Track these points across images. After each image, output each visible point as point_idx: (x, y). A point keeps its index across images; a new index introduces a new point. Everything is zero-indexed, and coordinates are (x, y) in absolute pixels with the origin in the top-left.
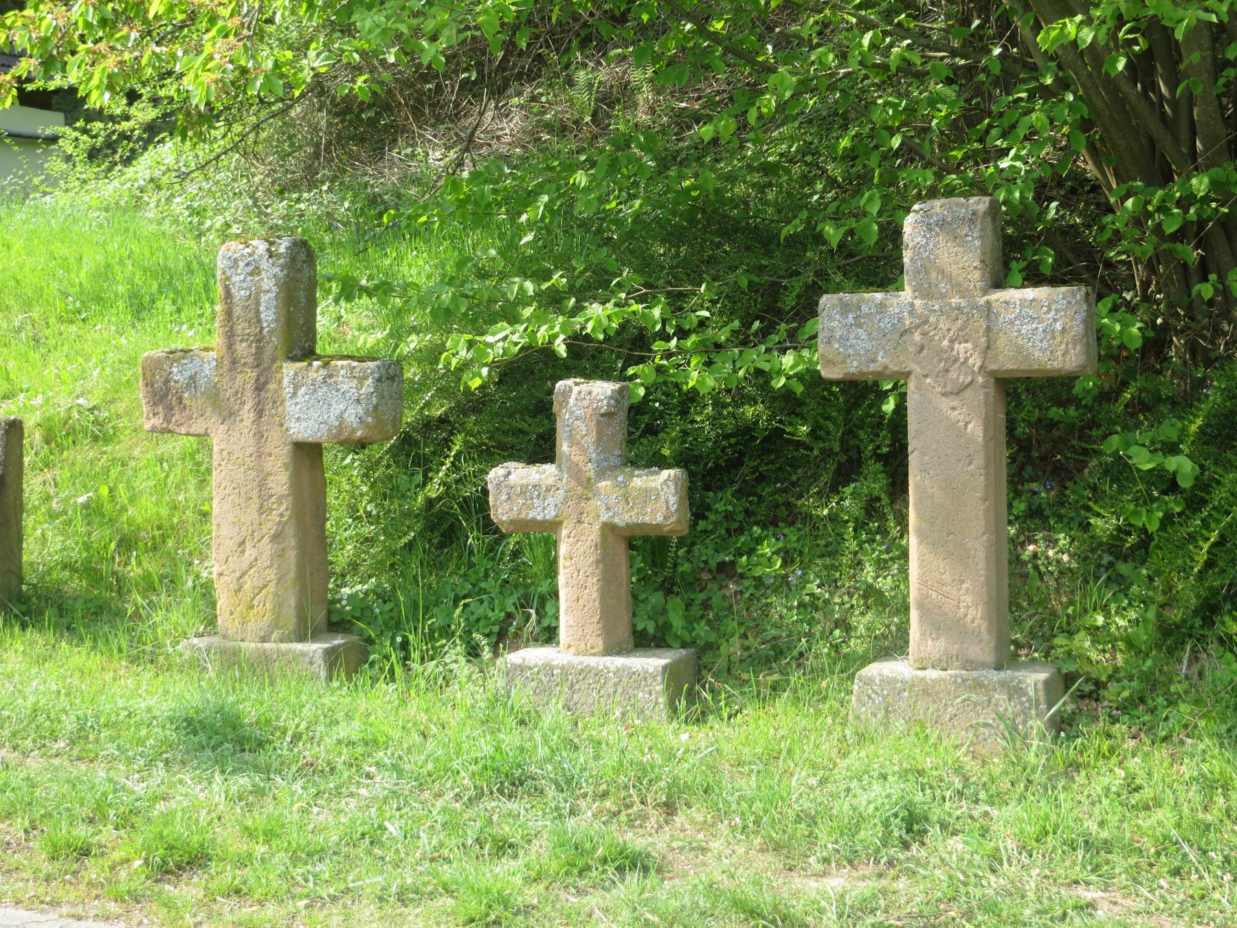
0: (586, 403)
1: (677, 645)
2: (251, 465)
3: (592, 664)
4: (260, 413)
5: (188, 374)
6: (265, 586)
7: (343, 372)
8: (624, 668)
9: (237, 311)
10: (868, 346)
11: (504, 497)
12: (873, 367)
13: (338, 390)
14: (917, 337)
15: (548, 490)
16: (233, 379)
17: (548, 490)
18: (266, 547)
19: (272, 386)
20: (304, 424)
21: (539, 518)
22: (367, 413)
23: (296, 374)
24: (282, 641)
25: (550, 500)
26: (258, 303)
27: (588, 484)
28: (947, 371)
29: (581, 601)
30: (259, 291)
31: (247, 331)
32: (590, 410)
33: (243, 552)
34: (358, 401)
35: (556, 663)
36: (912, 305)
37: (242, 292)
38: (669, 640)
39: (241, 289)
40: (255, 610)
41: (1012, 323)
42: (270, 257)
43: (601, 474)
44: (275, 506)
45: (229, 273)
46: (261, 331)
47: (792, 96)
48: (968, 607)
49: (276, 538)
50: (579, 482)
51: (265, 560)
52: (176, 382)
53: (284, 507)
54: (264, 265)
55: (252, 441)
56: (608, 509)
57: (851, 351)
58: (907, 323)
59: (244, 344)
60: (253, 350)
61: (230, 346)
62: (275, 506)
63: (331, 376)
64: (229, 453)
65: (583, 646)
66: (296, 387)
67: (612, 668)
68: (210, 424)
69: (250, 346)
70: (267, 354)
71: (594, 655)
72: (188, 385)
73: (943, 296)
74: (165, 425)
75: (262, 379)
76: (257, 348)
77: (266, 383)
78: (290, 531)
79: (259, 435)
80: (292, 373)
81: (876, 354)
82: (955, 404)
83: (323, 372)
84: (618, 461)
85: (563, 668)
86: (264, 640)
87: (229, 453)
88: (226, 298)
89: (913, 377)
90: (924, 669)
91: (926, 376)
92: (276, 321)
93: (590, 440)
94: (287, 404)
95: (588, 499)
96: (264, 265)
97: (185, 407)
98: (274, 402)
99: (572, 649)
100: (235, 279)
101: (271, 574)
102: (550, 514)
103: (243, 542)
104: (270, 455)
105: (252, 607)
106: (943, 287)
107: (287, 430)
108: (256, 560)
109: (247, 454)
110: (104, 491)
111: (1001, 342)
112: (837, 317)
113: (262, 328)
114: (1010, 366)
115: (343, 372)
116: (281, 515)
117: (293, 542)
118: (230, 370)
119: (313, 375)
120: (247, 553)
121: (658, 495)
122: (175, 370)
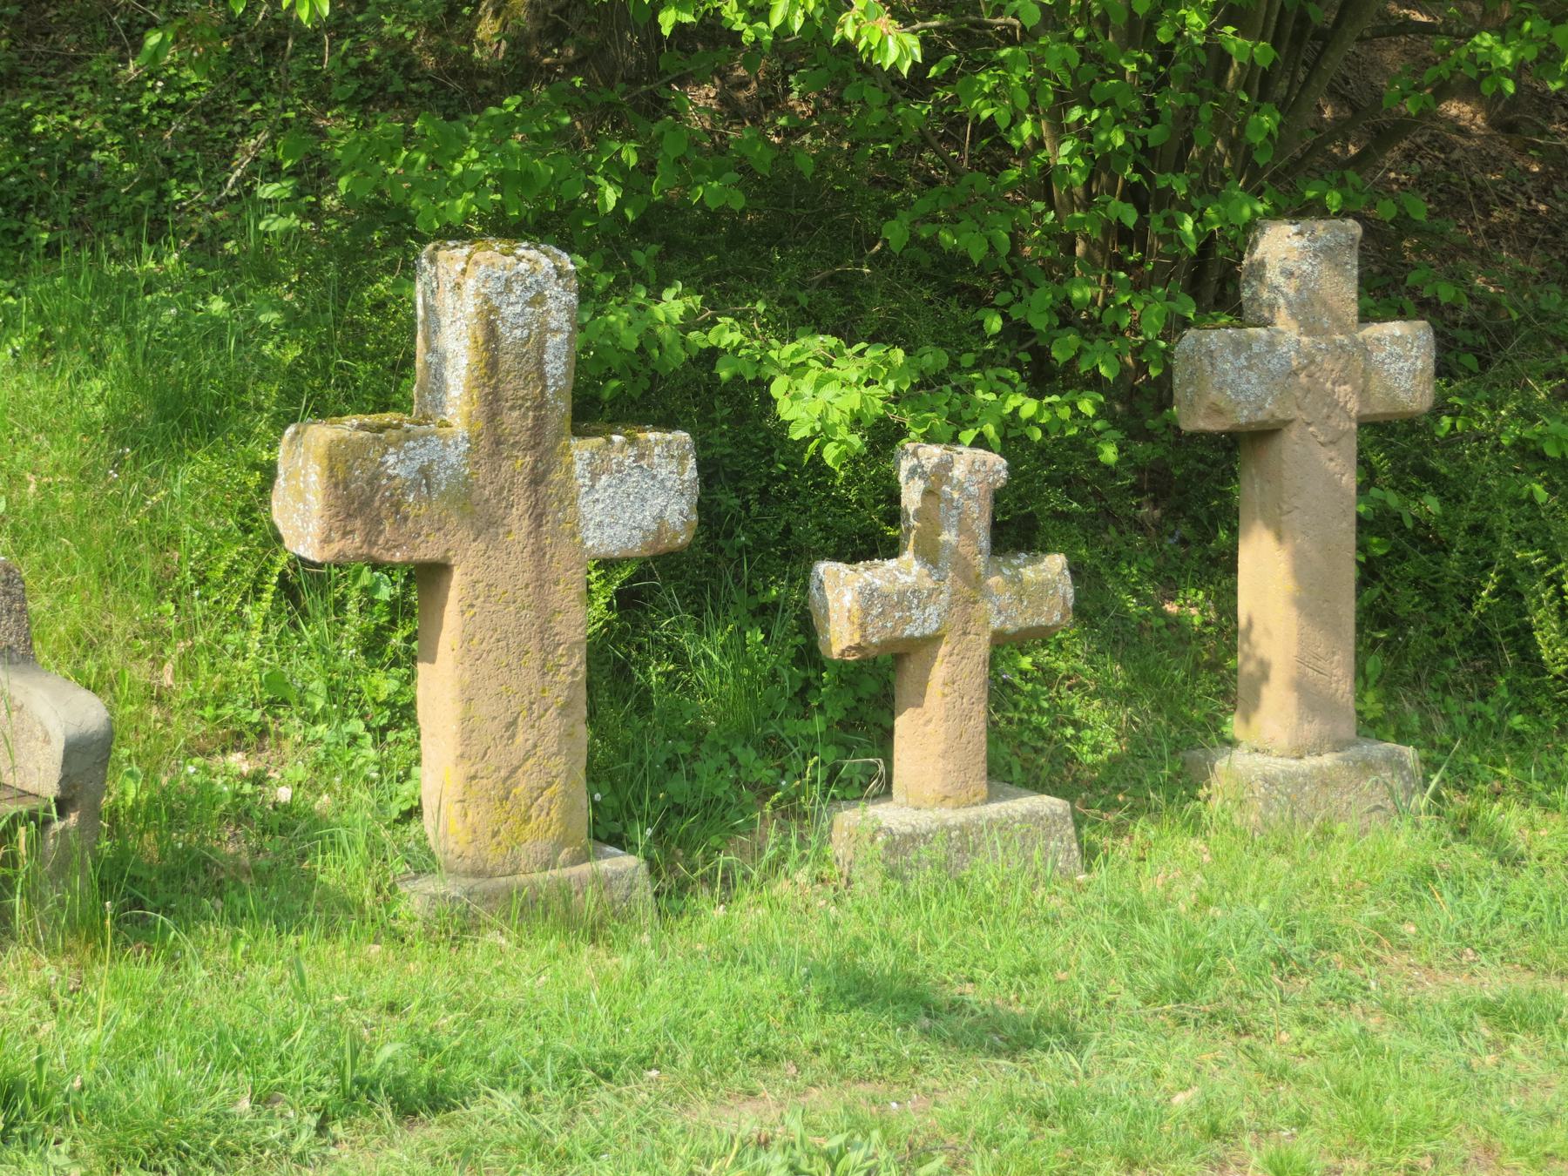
0: (981, 476)
2: (527, 601)
4: (538, 519)
5: (416, 464)
6: (550, 785)
7: (657, 450)
9: (507, 361)
10: (1258, 390)
12: (1261, 416)
13: (654, 477)
14: (1303, 378)
15: (930, 596)
16: (496, 469)
18: (552, 723)
19: (556, 476)
20: (609, 532)
21: (917, 634)
23: (593, 455)
25: (930, 609)
27: (976, 583)
28: (1329, 417)
29: (964, 740)
30: (545, 329)
31: (521, 393)
33: (512, 737)
36: (1299, 342)
37: (518, 332)
39: (514, 326)
40: (533, 824)
41: (1383, 362)
42: (560, 276)
44: (563, 661)
45: (495, 302)
46: (542, 392)
47: (246, 9)
48: (1338, 682)
49: (565, 709)
50: (966, 580)
51: (550, 743)
52: (390, 478)
53: (577, 659)
54: (553, 289)
57: (1242, 398)
58: (1294, 363)
59: (516, 414)
60: (530, 422)
62: (563, 661)
63: (641, 456)
64: (489, 586)
66: (595, 477)
68: (453, 542)
69: (525, 416)
70: (549, 429)
72: (416, 485)
73: (1326, 332)
74: (365, 550)
76: (536, 418)
79: (539, 552)
80: (587, 455)
81: (1265, 400)
82: (1333, 454)
83: (632, 451)
85: (961, 828)
86: (546, 866)
87: (489, 586)
88: (487, 342)
89: (1296, 425)
90: (1301, 757)
91: (1309, 424)
92: (566, 375)
95: (975, 602)
97: (406, 519)
98: (561, 501)
99: (950, 802)
100: (507, 311)
102: (931, 627)
104: (557, 583)
106: (1326, 321)
107: (583, 542)
108: (535, 746)
109: (520, 584)
111: (1375, 382)
112: (1231, 358)
113: (545, 387)
114: (1380, 410)
116: (574, 673)
120: (519, 739)
122: (391, 460)
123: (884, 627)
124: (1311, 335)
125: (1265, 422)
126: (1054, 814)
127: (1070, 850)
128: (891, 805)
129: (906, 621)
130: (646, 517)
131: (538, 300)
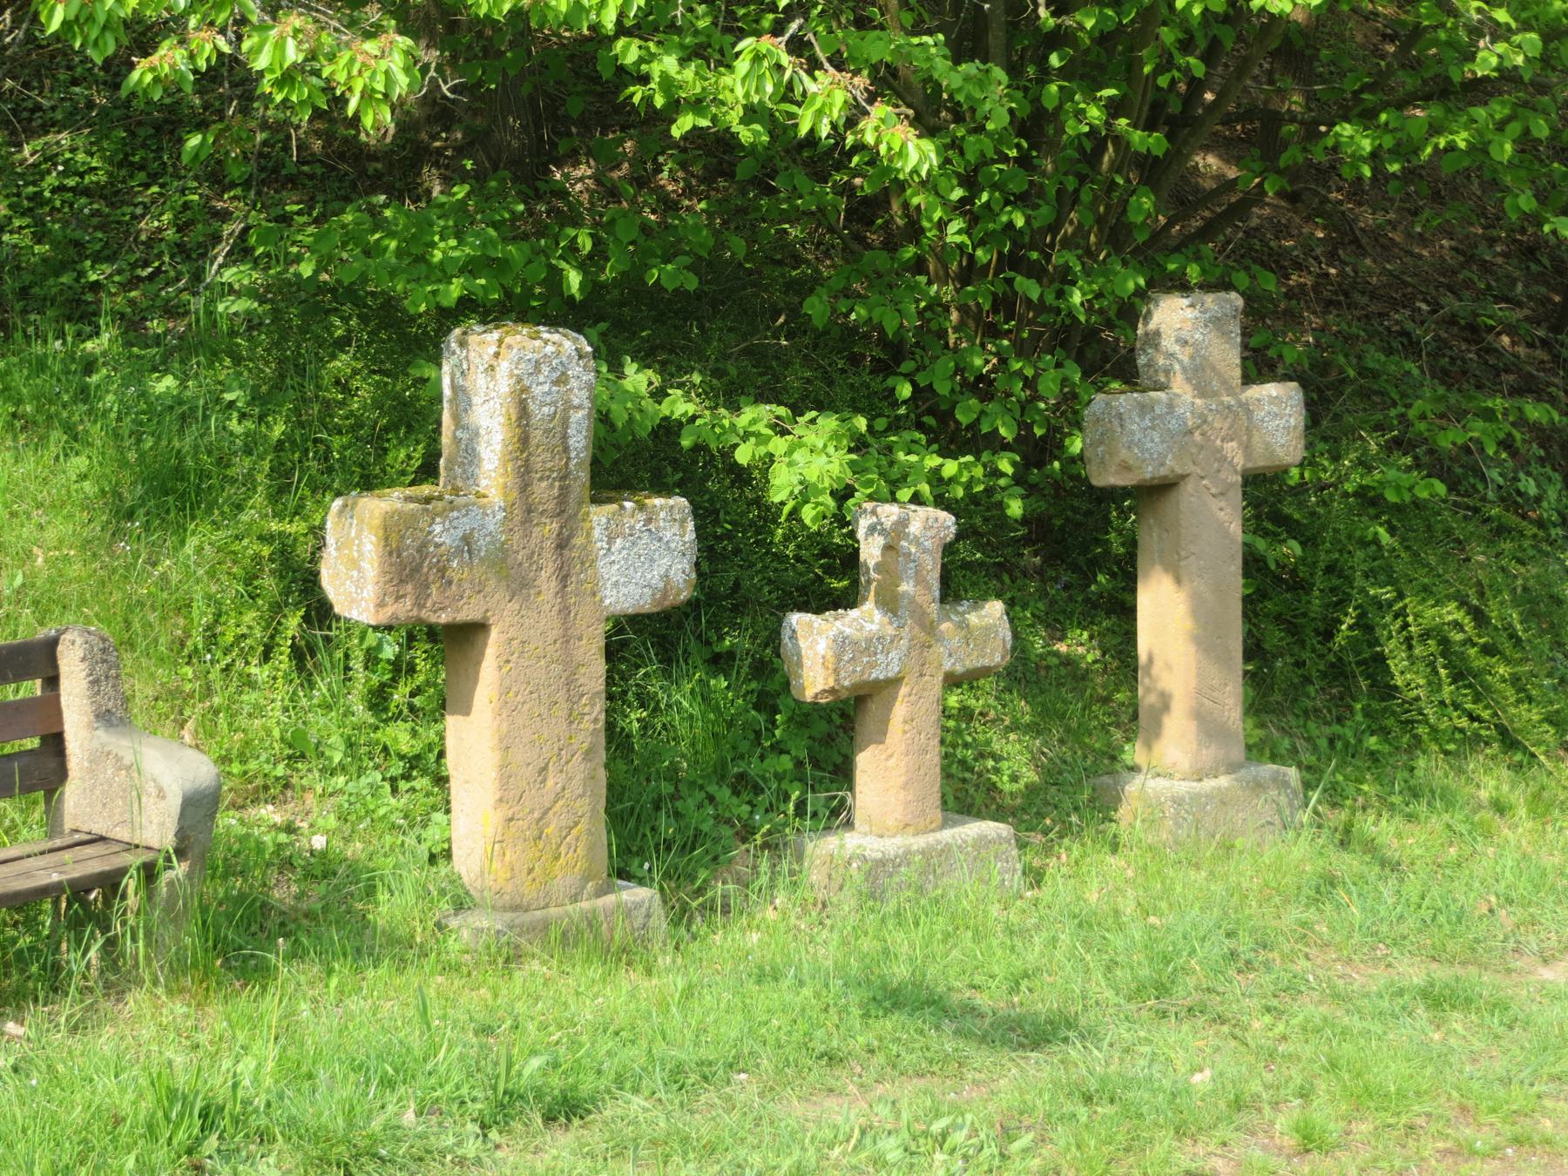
0: (934, 531)
4: (564, 580)
6: (576, 824)
7: (662, 515)
9: (537, 436)
10: (1161, 448)
12: (1163, 472)
13: (660, 539)
16: (527, 535)
18: (578, 768)
19: (578, 541)
20: (624, 590)
27: (930, 628)
30: (569, 406)
31: (549, 465)
32: (936, 540)
33: (544, 781)
37: (546, 410)
40: (562, 861)
42: (580, 357)
44: (587, 710)
45: (527, 383)
46: (567, 464)
49: (589, 754)
50: (922, 626)
51: (577, 786)
52: (438, 546)
53: (598, 708)
54: (575, 370)
55: (557, 623)
59: (544, 484)
60: (556, 492)
61: (525, 487)
62: (587, 710)
63: (649, 521)
69: (551, 486)
71: (933, 831)
72: (459, 551)
74: (415, 613)
75: (566, 533)
79: (565, 611)
80: (604, 520)
82: (1223, 504)
83: (641, 516)
85: (923, 853)
86: (575, 899)
88: (520, 418)
90: (1200, 780)
92: (586, 448)
97: (450, 583)
98: (583, 563)
99: (911, 830)
100: (537, 390)
103: (545, 769)
104: (580, 639)
105: (557, 858)
106: (1216, 384)
107: (602, 601)
109: (550, 640)
111: (1256, 439)
113: (569, 459)
116: (596, 720)
118: (523, 523)
120: (550, 783)
123: (854, 671)
124: (1202, 398)
125: (1166, 477)
126: (1000, 837)
129: (872, 665)
130: (655, 576)
131: (562, 380)
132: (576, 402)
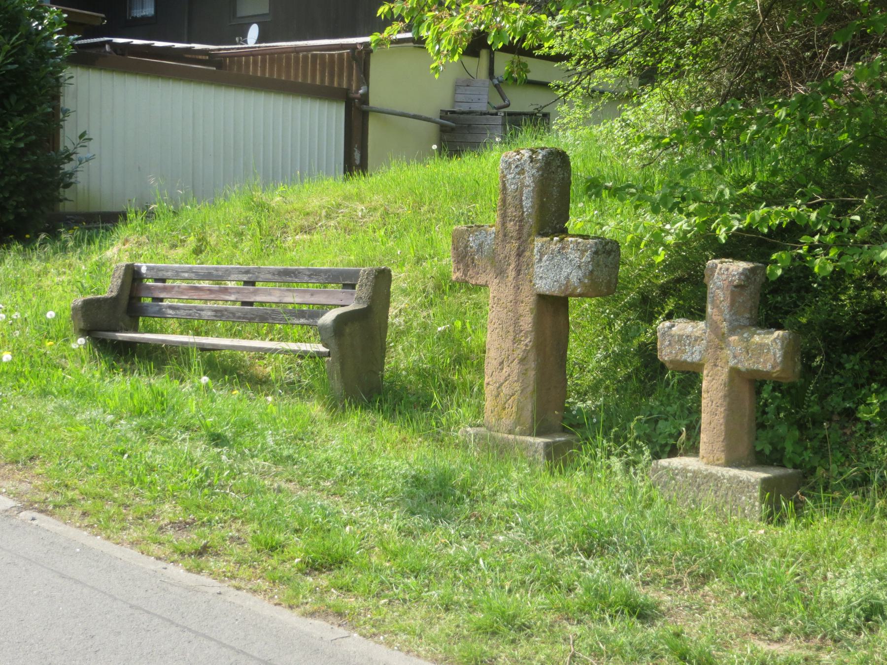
0: (724, 277)
1: (789, 466)
3: (714, 472)
4: (518, 272)
6: (513, 395)
7: (571, 246)
8: (736, 477)
9: (509, 199)
11: (667, 343)
13: (567, 259)
15: (696, 340)
17: (696, 340)
19: (527, 254)
20: (544, 281)
21: (689, 360)
22: (585, 276)
23: (542, 246)
24: (521, 434)
26: (521, 195)
27: (723, 337)
29: (712, 426)
32: (726, 282)
33: (502, 369)
34: (579, 266)
35: (690, 468)
38: (785, 462)
39: (512, 184)
42: (531, 162)
43: (733, 331)
49: (522, 361)
50: (717, 336)
51: (514, 377)
53: (528, 340)
55: (512, 291)
56: (735, 357)
61: (504, 224)
65: (711, 458)
67: (727, 476)
69: (515, 224)
70: (526, 230)
71: (718, 465)
75: (522, 248)
77: (523, 251)
78: (532, 356)
79: (517, 288)
83: (559, 245)
84: (747, 322)
85: (694, 472)
92: (532, 207)
93: (726, 304)
94: (536, 266)
95: (722, 349)
96: (527, 167)
98: (528, 265)
99: (705, 460)
101: (517, 387)
102: (696, 357)
104: (522, 302)
105: (504, 409)
107: (534, 285)
108: (509, 375)
110: (458, 324)
115: (571, 246)
116: (526, 345)
117: (533, 366)
118: (502, 241)
119: (553, 246)
120: (504, 371)
121: (768, 349)
122: (471, 239)
123: (671, 353)
127: (754, 506)
128: (697, 459)
129: (684, 352)
132: (527, 183)
